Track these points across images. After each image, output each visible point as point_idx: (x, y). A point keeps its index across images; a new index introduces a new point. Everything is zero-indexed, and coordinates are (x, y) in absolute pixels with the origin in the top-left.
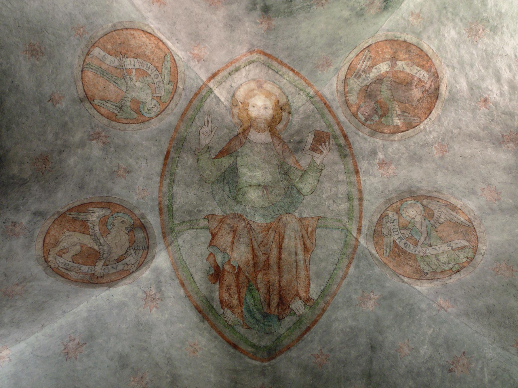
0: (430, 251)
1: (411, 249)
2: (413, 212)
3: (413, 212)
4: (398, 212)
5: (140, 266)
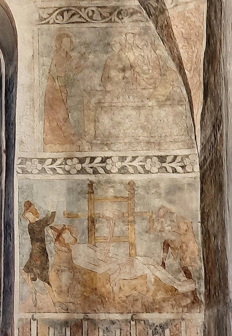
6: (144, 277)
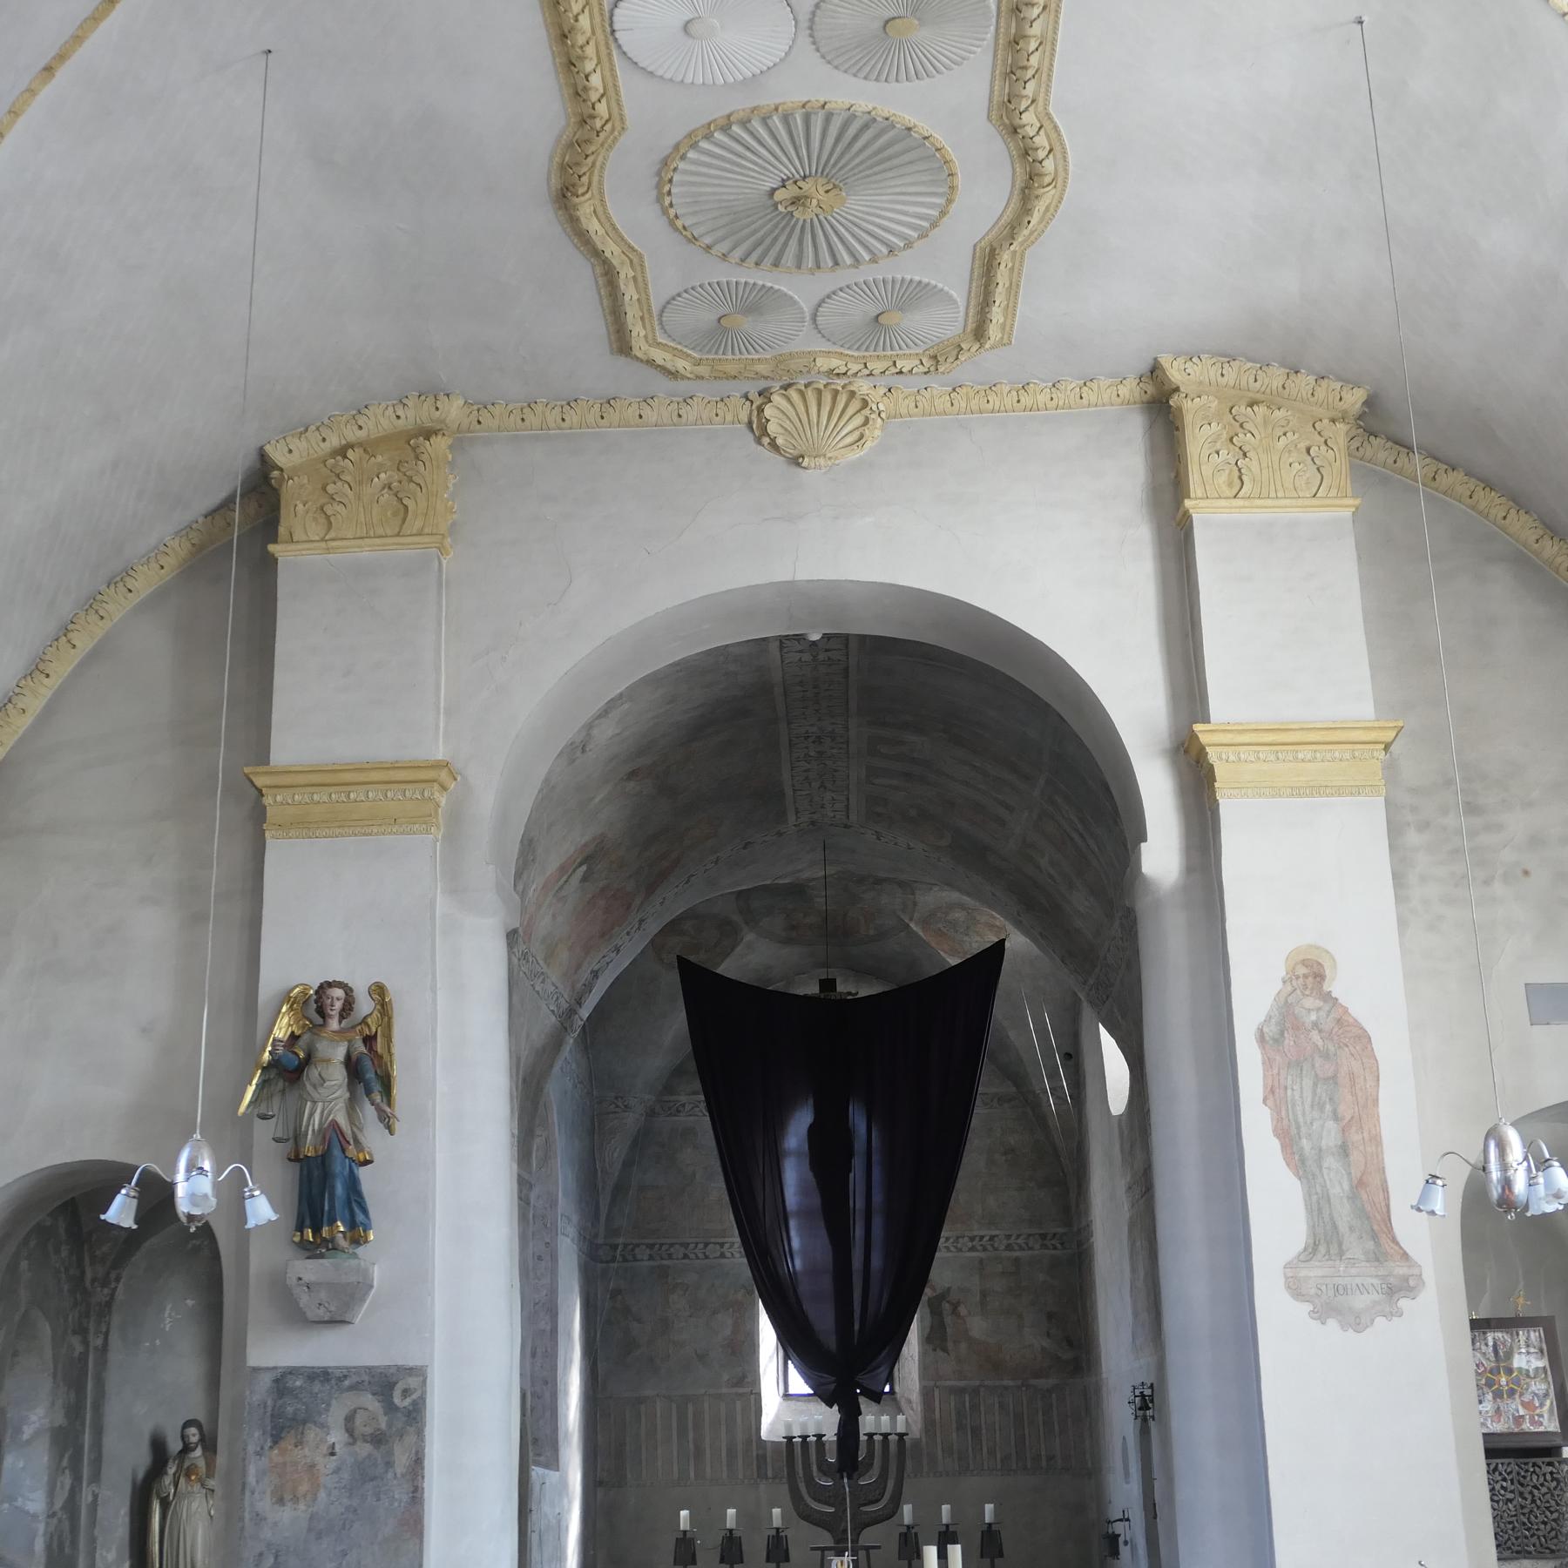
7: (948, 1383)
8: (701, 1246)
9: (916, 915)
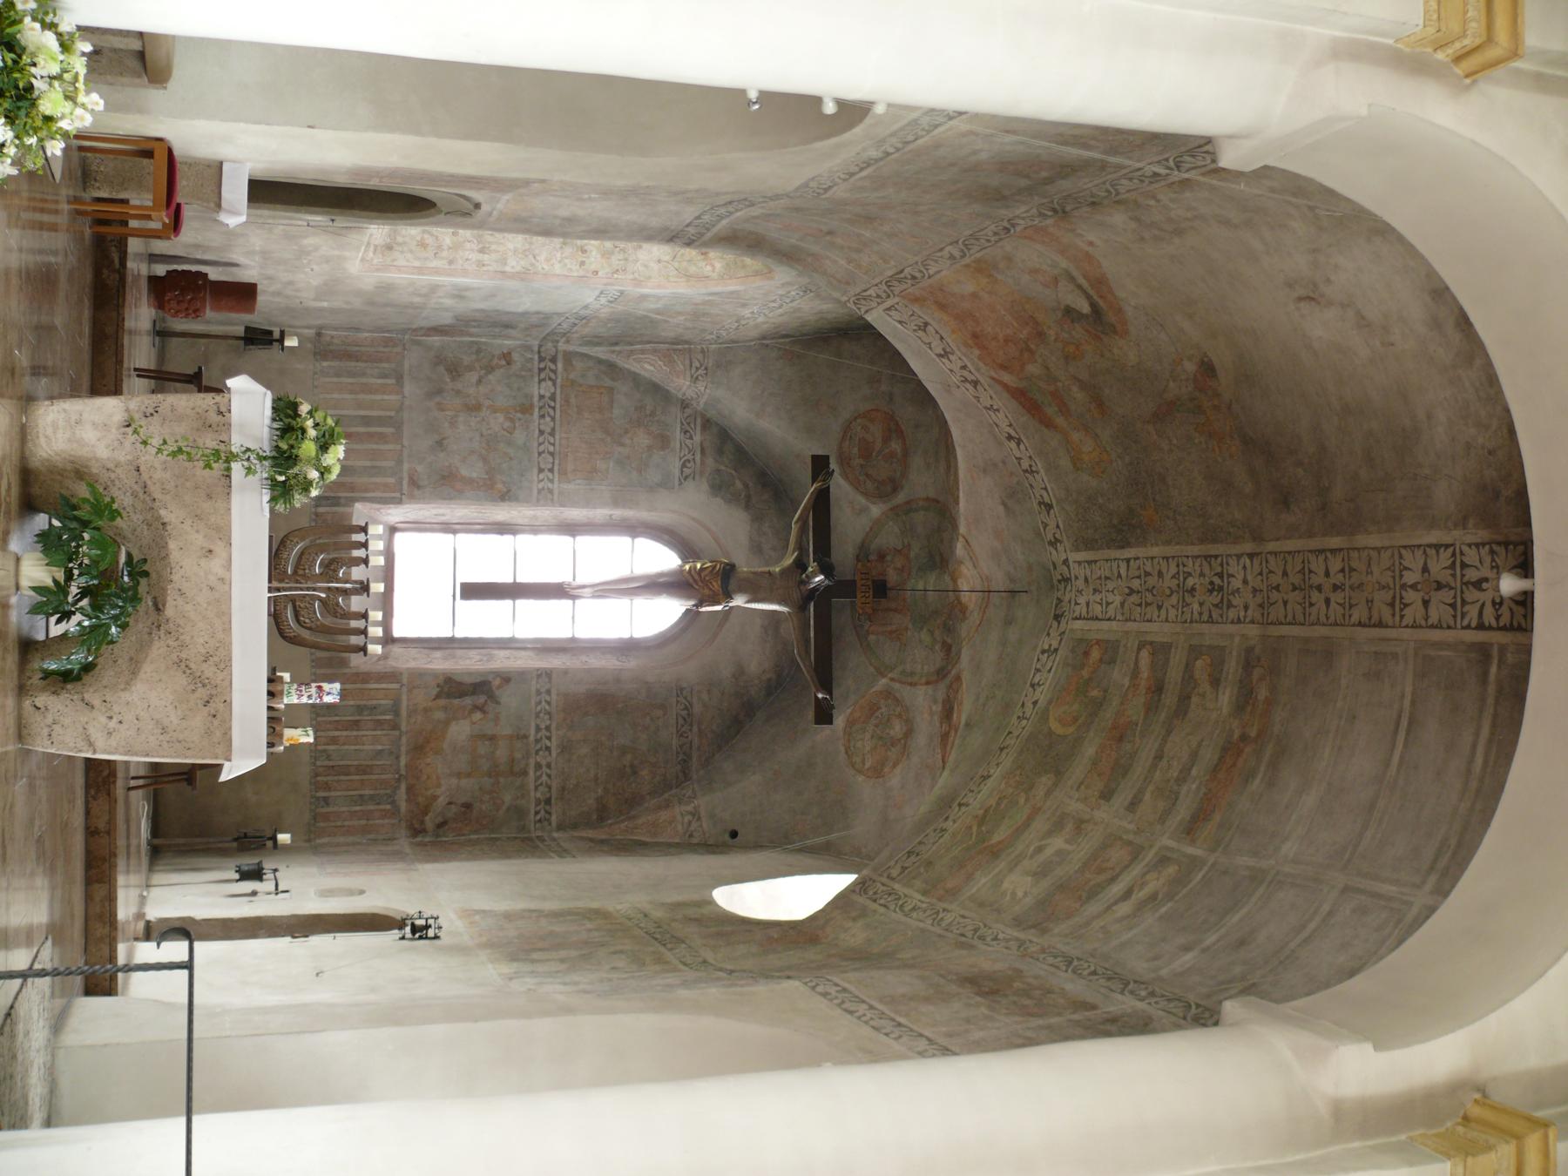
0: (868, 736)
1: (873, 721)
2: (897, 729)
3: (897, 729)
4: (900, 716)
5: (866, 494)
6: (439, 786)
7: (404, 697)
8: (551, 449)
9: (897, 686)
